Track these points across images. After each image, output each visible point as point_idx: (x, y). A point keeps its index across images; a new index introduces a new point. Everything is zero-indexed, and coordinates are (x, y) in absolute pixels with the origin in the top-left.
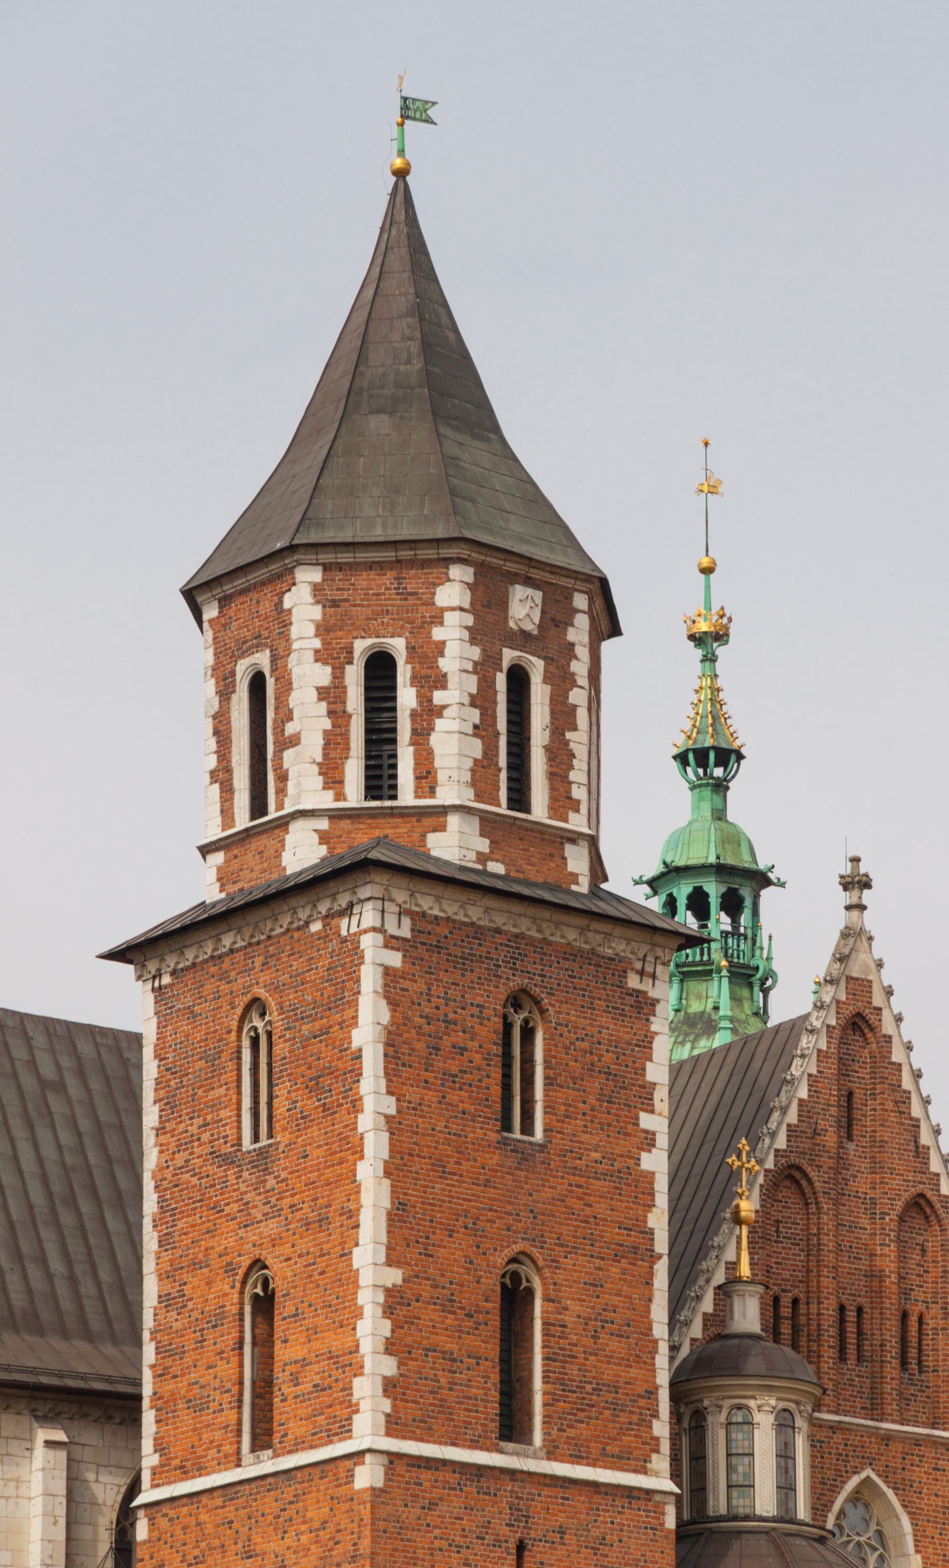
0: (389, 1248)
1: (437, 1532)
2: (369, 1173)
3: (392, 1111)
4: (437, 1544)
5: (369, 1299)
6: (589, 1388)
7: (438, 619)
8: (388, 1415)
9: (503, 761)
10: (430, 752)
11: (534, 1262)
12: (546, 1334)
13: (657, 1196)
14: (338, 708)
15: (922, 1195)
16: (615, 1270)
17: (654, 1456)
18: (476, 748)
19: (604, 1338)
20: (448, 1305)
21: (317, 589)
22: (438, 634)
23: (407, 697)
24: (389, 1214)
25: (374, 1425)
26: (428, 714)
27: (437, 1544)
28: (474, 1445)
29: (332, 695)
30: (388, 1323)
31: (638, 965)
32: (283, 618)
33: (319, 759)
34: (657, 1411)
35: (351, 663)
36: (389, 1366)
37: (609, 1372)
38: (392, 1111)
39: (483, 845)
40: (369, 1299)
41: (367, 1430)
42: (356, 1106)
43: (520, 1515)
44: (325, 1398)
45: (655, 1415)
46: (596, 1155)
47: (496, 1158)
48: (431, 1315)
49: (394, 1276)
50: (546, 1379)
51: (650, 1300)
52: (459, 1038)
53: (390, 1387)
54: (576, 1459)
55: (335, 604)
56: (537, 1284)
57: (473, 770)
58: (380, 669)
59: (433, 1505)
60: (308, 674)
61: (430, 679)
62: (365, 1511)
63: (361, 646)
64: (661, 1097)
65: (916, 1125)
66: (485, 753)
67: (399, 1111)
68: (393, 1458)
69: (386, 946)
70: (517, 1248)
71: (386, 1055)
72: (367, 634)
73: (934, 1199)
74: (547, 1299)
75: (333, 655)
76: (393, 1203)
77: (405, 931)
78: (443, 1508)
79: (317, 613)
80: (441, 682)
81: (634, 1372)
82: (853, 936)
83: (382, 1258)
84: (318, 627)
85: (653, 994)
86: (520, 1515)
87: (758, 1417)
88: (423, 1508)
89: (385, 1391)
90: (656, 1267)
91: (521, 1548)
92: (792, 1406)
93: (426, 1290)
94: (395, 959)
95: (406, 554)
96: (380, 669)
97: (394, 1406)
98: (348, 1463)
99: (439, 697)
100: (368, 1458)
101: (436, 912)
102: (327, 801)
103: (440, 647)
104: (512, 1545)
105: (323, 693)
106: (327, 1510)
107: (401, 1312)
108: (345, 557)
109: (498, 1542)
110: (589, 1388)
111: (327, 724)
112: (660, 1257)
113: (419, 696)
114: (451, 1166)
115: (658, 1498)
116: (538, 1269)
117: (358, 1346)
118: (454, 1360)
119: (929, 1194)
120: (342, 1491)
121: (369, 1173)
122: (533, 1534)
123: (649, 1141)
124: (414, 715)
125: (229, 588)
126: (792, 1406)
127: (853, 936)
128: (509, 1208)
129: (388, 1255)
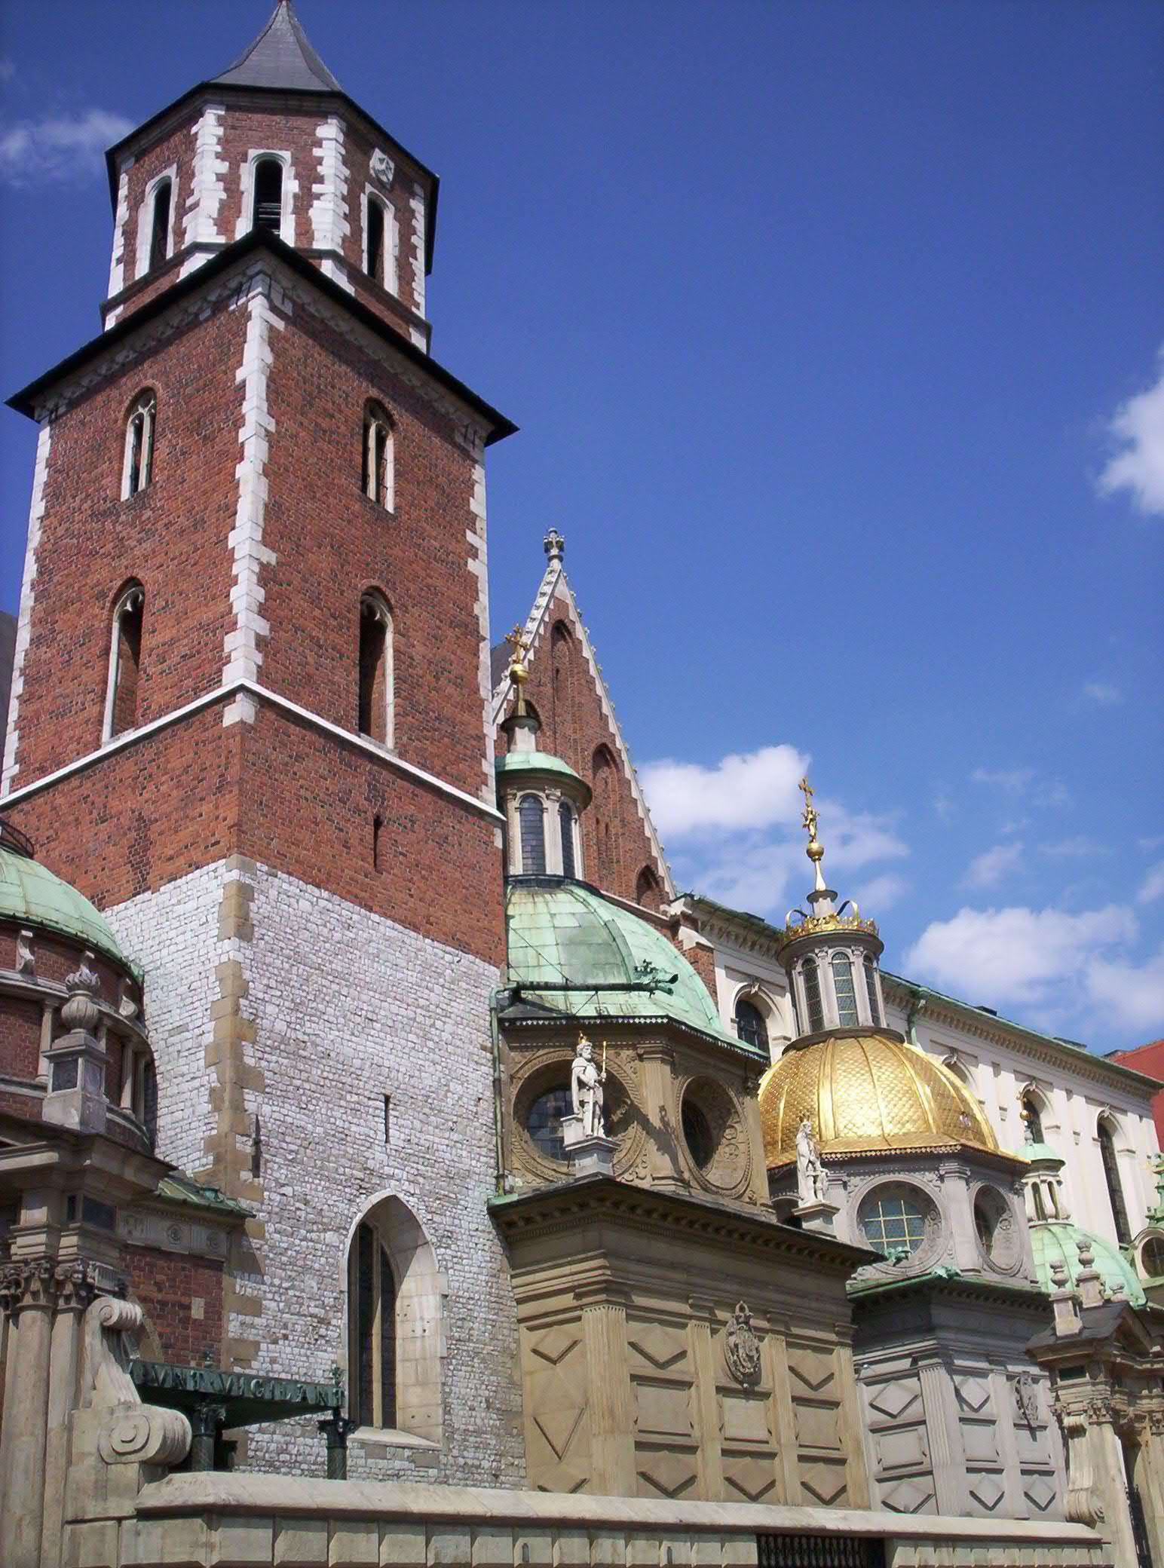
0: (264, 531)
2: (249, 474)
3: (272, 428)
4: (302, 792)
5: (244, 571)
7: (319, 143)
8: (259, 667)
9: (365, 246)
10: (309, 222)
11: (387, 601)
12: (396, 658)
13: (480, 594)
14: (233, 187)
18: (347, 229)
19: (443, 681)
20: (315, 601)
21: (219, 118)
22: (317, 152)
23: (290, 186)
24: (266, 506)
25: (246, 670)
26: (305, 200)
27: (302, 792)
28: (336, 722)
29: (230, 182)
30: (263, 591)
32: (191, 141)
33: (215, 216)
35: (245, 161)
36: (263, 627)
37: (448, 710)
40: (244, 571)
41: (240, 668)
42: (239, 422)
44: (194, 662)
48: (299, 602)
49: (270, 557)
50: (397, 694)
53: (261, 643)
54: (423, 767)
55: (234, 128)
56: (389, 619)
58: (269, 178)
59: (299, 758)
60: (208, 166)
61: (309, 174)
62: (234, 745)
63: (253, 153)
64: (481, 525)
67: (278, 432)
68: (264, 702)
70: (374, 582)
72: (258, 146)
74: (397, 631)
75: (232, 152)
77: (288, 309)
78: (308, 763)
79: (220, 131)
80: (320, 180)
81: (466, 716)
83: (259, 536)
84: (219, 139)
86: (376, 793)
87: (546, 804)
88: (291, 757)
89: (258, 646)
91: (378, 823)
92: (570, 802)
94: (280, 325)
95: (293, 103)
96: (269, 178)
98: (216, 708)
99: (316, 188)
100: (239, 696)
101: (312, 310)
102: (222, 240)
103: (320, 161)
105: (220, 178)
106: (192, 755)
108: (244, 101)
109: (357, 810)
111: (224, 196)
113: (301, 187)
116: (391, 609)
117: (231, 607)
118: (320, 647)
120: (215, 731)
121: (249, 474)
124: (295, 196)
125: (144, 142)
126: (570, 802)
129: (263, 537)
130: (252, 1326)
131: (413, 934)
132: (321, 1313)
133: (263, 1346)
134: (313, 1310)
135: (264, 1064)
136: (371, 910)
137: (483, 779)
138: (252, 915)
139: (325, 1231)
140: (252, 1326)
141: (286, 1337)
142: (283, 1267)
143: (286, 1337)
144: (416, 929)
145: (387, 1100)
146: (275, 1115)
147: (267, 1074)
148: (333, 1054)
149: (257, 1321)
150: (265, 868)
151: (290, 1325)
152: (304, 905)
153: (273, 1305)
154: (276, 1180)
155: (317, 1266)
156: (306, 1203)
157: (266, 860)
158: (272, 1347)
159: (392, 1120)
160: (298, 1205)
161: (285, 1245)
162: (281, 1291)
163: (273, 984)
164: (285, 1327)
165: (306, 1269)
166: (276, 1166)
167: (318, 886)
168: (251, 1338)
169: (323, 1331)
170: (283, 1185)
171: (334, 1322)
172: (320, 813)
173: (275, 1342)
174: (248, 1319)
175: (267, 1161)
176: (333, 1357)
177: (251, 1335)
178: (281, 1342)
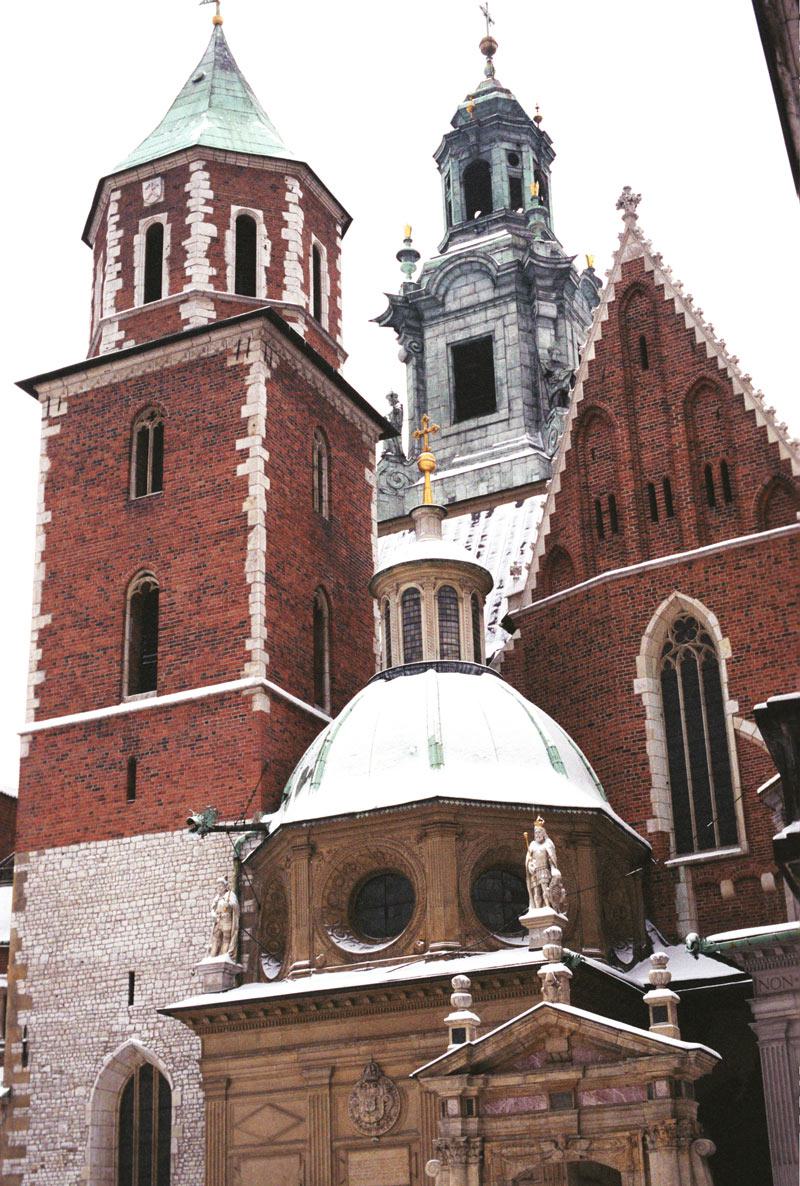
1: (66, 772)
3: (49, 520)
6: (192, 638)
15: (704, 378)
16: (215, 552)
17: (247, 665)
31: (235, 350)
34: (250, 633)
38: (49, 520)
39: (122, 335)
43: (133, 742)
45: (248, 635)
46: (202, 483)
47: (123, 517)
51: (244, 560)
52: (98, 455)
57: (116, 298)
65: (692, 331)
66: (125, 284)
69: (50, 425)
71: (46, 488)
73: (714, 376)
76: (46, 575)
82: (631, 233)
85: (247, 361)
90: (249, 536)
93: (68, 620)
97: (41, 703)
104: (125, 764)
107: (49, 642)
110: (192, 638)
112: (253, 527)
114: (88, 537)
115: (245, 693)
119: (709, 374)
122: (141, 751)
123: (244, 454)
127: (631, 233)
128: (133, 544)
130: (20, 1165)
131: (163, 835)
132: (70, 1144)
133: (26, 1177)
134: (64, 1144)
135: (32, 989)
136: (122, 835)
137: (248, 657)
138: (25, 891)
139: (75, 1088)
140: (20, 1165)
141: (43, 1167)
142: (43, 1121)
143: (43, 1167)
144: (163, 828)
145: (132, 975)
146: (40, 1021)
147: (34, 995)
148: (86, 961)
149: (23, 1161)
150: (35, 853)
151: (46, 1159)
152: (66, 863)
153: (34, 1148)
154: (39, 1064)
155: (67, 1114)
156: (61, 1072)
157: (33, 847)
158: (32, 1176)
159: (136, 988)
160: (54, 1076)
161: (44, 1106)
162: (41, 1137)
163: (40, 931)
164: (43, 1160)
165: (60, 1118)
166: (39, 1055)
167: (77, 842)
168: (18, 1172)
169: (71, 1157)
170: (43, 1066)
171: (80, 1148)
172: (80, 787)
173: (35, 1171)
174: (17, 1161)
175: (34, 1053)
176: (77, 1173)
177: (17, 1171)
178: (39, 1171)
